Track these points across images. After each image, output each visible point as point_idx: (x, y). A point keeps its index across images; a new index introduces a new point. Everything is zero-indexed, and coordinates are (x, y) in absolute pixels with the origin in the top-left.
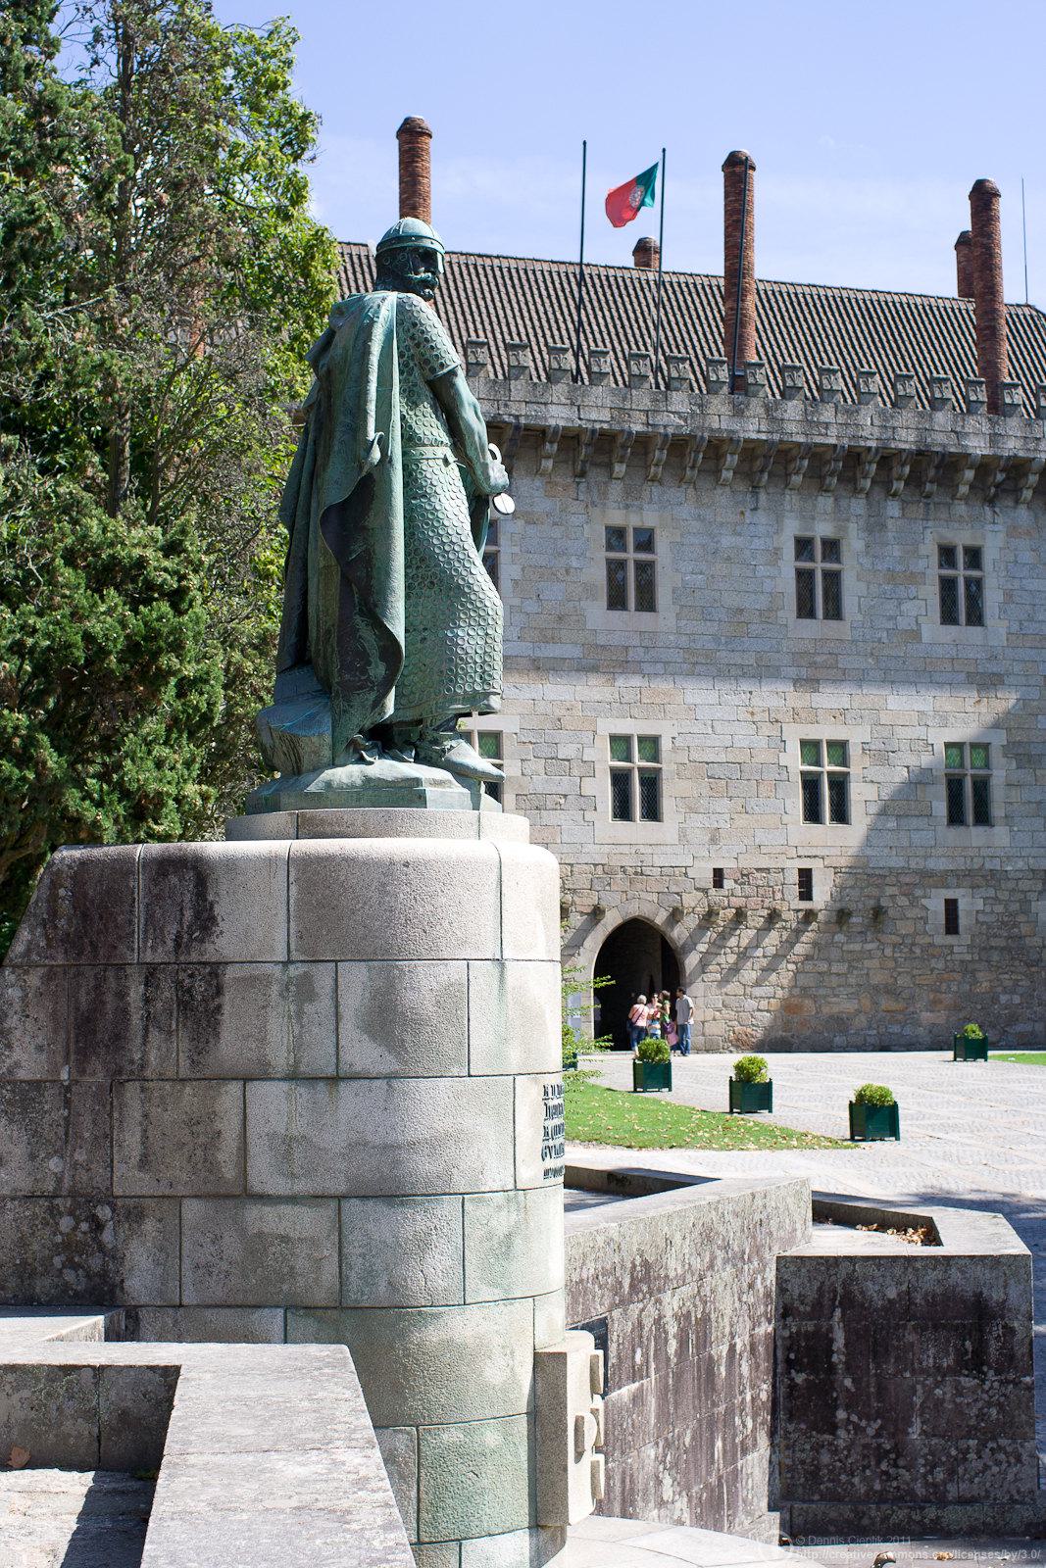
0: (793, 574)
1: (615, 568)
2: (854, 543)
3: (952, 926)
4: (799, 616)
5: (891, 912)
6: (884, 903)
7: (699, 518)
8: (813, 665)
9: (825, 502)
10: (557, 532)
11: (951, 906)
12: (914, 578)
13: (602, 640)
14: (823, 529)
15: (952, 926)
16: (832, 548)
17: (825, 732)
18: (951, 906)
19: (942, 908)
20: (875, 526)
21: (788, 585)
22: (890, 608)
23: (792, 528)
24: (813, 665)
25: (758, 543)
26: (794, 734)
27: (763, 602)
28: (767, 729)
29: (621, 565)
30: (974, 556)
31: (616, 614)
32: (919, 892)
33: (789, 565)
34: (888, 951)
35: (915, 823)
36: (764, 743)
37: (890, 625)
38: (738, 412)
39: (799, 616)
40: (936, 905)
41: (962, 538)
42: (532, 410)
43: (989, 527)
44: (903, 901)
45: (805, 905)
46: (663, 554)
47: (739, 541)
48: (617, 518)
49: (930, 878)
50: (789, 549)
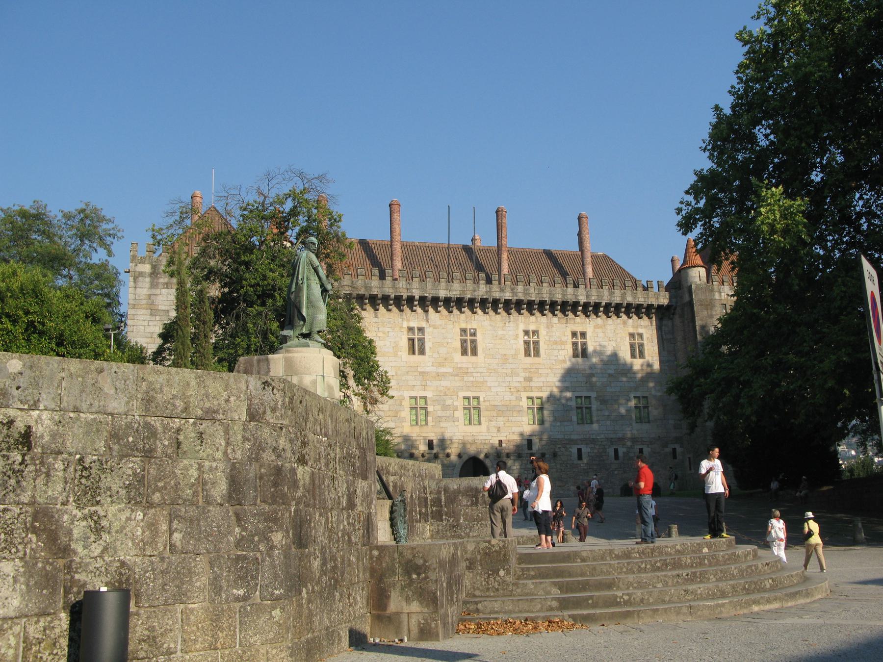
0: (522, 343)
1: (464, 342)
2: (543, 332)
3: (580, 457)
4: (525, 356)
5: (559, 453)
6: (557, 450)
7: (491, 325)
8: (530, 372)
9: (532, 318)
10: (444, 331)
11: (579, 451)
12: (563, 343)
13: (459, 366)
14: (532, 328)
15: (580, 457)
16: (536, 332)
17: (535, 394)
18: (579, 451)
19: (576, 451)
20: (549, 326)
21: (521, 346)
22: (556, 353)
23: (522, 327)
24: (530, 372)
25: (511, 333)
26: (524, 395)
27: (513, 352)
28: (515, 394)
29: (465, 341)
30: (583, 335)
31: (465, 357)
32: (568, 446)
33: (522, 338)
34: (559, 466)
35: (566, 423)
36: (514, 398)
37: (556, 358)
38: (502, 290)
39: (525, 356)
40: (574, 450)
41: (579, 329)
42: (434, 292)
43: (588, 325)
44: (563, 449)
45: (530, 452)
46: (479, 337)
47: (505, 332)
48: (463, 326)
49: (572, 442)
50: (521, 334)
